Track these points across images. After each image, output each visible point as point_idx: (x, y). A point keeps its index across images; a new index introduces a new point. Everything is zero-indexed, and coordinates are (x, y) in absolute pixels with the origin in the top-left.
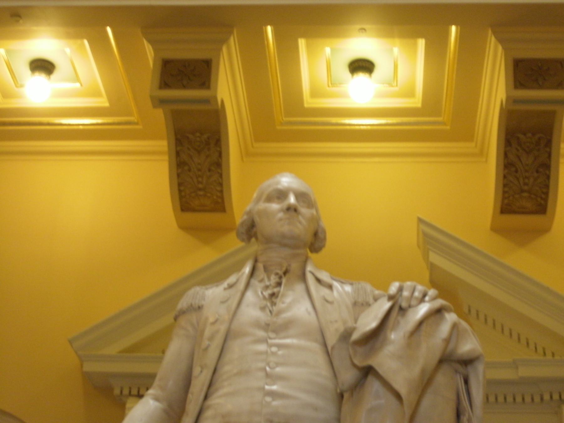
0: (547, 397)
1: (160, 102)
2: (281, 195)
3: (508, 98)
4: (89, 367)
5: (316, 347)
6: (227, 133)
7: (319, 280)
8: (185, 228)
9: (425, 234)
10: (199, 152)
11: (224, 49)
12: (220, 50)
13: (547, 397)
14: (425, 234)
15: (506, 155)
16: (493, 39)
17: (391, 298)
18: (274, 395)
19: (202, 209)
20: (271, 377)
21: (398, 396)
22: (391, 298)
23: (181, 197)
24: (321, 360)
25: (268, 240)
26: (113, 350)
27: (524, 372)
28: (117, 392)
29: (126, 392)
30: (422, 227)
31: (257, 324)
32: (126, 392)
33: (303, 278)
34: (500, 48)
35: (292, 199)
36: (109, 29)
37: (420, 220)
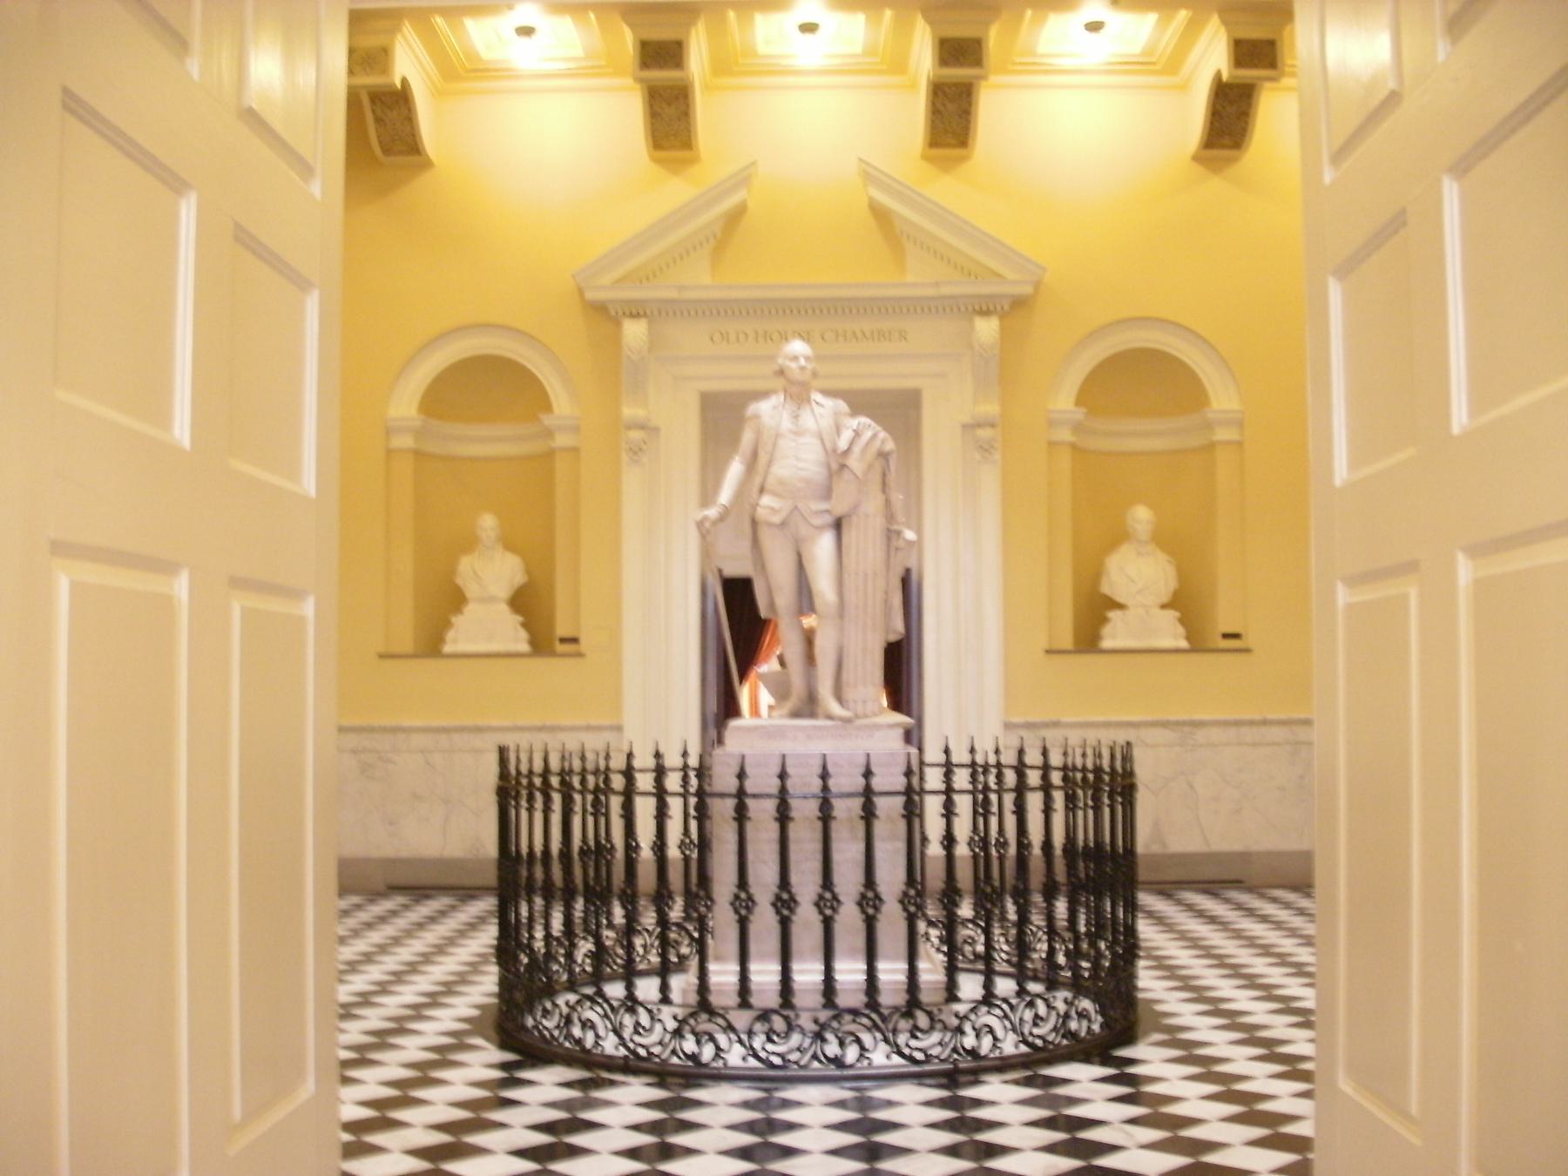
0: (963, 309)
1: (640, 80)
2: (795, 358)
3: (934, 76)
4: (589, 295)
5: (816, 442)
6: (693, 93)
7: (817, 403)
8: (657, 161)
9: (865, 172)
10: (669, 104)
11: (693, 32)
12: (688, 33)
13: (963, 309)
14: (865, 172)
15: (933, 104)
16: (922, 20)
17: (854, 430)
18: (801, 469)
19: (672, 147)
20: (798, 459)
21: (857, 477)
22: (854, 430)
23: (654, 137)
24: (819, 448)
25: (791, 382)
26: (606, 280)
27: (946, 290)
28: (613, 313)
29: (620, 313)
30: (863, 165)
31: (791, 431)
32: (620, 313)
33: (809, 401)
34: (928, 29)
35: (802, 362)
36: (592, 16)
37: (860, 160)
